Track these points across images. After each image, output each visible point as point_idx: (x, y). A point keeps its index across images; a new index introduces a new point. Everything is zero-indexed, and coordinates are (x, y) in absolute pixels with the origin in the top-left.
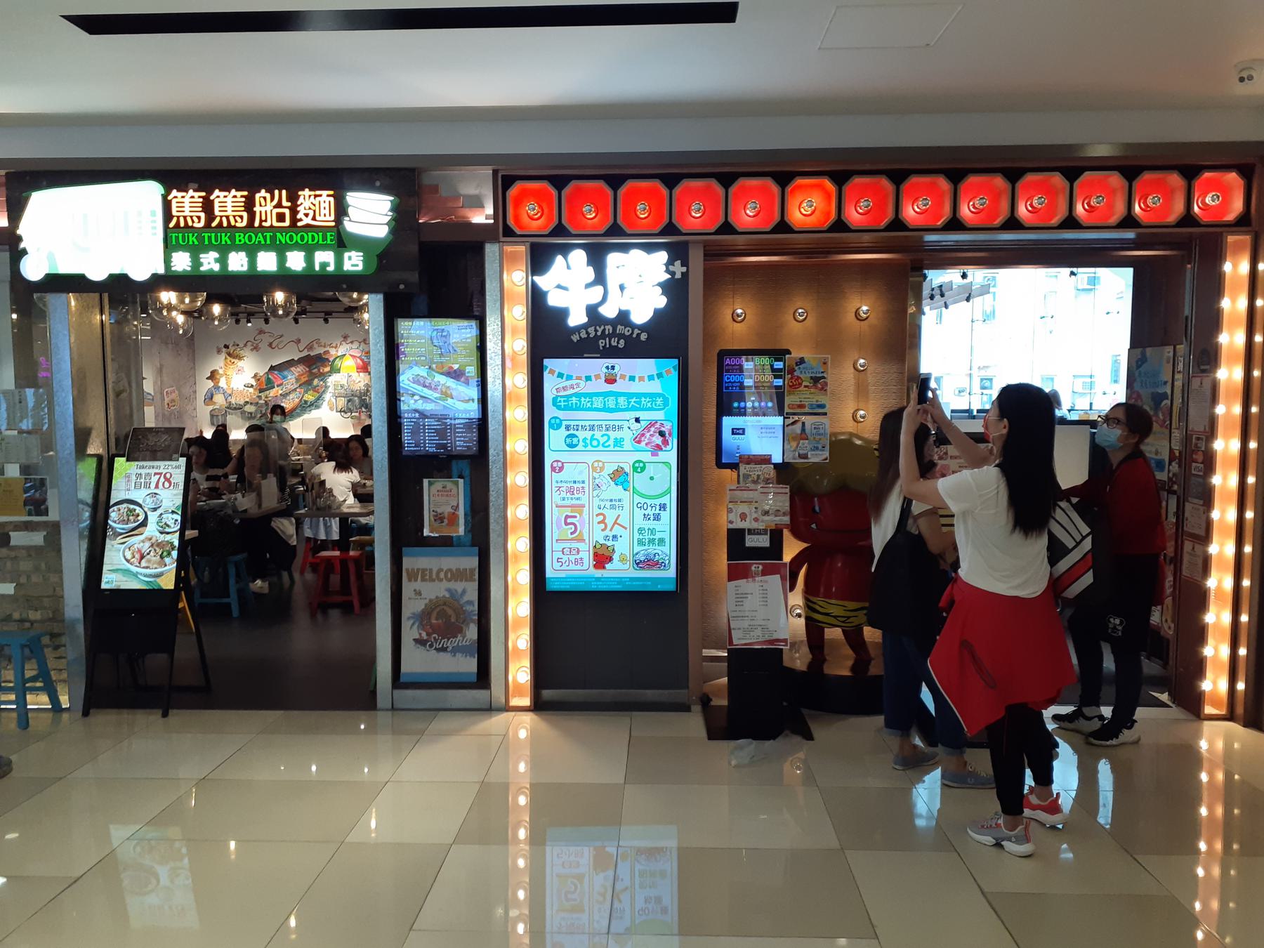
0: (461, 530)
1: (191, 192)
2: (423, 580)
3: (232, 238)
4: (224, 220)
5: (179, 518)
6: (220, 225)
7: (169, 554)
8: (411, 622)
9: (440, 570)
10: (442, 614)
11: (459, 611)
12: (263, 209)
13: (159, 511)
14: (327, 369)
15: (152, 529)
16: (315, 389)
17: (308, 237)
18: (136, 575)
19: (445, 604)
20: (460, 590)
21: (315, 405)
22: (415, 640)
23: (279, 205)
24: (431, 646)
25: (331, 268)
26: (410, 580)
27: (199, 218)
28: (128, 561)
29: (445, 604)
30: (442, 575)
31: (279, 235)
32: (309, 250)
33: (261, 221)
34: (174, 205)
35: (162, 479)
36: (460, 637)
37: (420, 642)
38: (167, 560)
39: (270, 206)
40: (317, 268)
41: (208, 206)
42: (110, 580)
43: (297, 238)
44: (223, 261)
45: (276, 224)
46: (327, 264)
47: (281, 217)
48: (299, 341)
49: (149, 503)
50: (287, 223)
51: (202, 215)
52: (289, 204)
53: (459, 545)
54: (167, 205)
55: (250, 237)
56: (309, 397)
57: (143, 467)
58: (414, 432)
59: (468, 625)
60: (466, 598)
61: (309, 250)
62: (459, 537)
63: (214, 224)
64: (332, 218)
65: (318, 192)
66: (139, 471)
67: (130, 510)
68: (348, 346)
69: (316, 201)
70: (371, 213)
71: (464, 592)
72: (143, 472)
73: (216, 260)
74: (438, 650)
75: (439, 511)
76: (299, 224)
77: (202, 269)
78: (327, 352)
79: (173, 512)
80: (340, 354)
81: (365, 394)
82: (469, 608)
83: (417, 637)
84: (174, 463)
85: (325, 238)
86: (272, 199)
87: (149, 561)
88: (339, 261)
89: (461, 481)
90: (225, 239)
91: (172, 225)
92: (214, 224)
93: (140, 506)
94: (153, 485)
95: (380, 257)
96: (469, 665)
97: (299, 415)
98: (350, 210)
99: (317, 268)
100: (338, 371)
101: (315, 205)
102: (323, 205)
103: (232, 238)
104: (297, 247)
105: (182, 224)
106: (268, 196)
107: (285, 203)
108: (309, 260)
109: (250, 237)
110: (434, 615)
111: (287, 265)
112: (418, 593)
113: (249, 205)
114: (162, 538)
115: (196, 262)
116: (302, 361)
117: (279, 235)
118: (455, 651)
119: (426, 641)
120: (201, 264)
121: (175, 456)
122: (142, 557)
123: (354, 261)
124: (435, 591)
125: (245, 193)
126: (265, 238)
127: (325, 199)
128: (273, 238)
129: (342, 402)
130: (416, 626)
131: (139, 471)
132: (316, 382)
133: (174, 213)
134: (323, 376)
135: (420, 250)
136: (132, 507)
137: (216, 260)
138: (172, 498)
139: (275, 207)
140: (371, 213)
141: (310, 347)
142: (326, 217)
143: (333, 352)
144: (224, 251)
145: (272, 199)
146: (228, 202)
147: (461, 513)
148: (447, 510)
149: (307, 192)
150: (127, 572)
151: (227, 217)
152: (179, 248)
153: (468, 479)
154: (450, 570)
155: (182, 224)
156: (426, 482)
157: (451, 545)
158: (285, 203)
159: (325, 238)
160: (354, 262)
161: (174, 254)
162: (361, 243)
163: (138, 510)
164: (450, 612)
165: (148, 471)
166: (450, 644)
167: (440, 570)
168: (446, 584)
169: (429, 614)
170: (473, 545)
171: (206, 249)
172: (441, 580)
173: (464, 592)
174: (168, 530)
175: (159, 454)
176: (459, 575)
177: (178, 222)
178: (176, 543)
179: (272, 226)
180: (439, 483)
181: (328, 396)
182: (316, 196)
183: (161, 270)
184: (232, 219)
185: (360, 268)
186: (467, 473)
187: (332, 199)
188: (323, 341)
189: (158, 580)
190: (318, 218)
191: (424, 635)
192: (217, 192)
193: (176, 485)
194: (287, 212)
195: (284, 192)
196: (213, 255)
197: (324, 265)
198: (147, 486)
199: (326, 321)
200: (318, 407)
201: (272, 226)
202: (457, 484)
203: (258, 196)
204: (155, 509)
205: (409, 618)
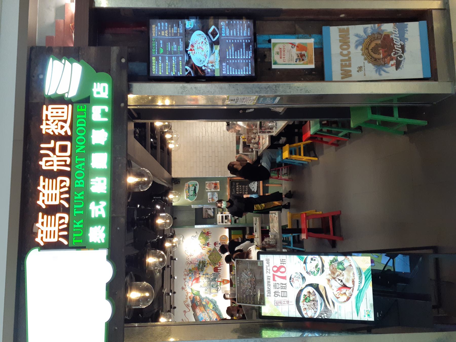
0: (311, 41)
1: (38, 225)
2: (350, 65)
3: (79, 190)
4: (63, 196)
5: (310, 257)
6: (67, 200)
7: (341, 263)
8: (382, 72)
9: (341, 54)
10: (375, 50)
11: (372, 38)
12: (56, 163)
13: (305, 275)
14: (198, 297)
15: (321, 280)
16: (207, 303)
17: (80, 126)
18: (360, 291)
19: (367, 49)
20: (357, 38)
21: (215, 304)
22: (397, 68)
23: (53, 150)
24: (401, 57)
25: (107, 109)
26: (351, 76)
27: (61, 218)
28: (348, 299)
29: (367, 49)
30: (345, 52)
31: (77, 151)
32: (91, 125)
33: (66, 165)
34: (48, 240)
35: (279, 274)
36: (393, 36)
37: (398, 65)
38: (346, 264)
39: (54, 158)
40: (106, 119)
41: (51, 210)
42: (366, 313)
43: (81, 136)
44: (97, 198)
45: (68, 153)
46: (103, 111)
47: (63, 149)
48: (185, 311)
49: (299, 284)
50: (68, 143)
51: (58, 215)
52: (53, 142)
53: (321, 43)
54: (49, 246)
55: (80, 175)
56: (211, 306)
57: (269, 291)
58: (237, 67)
59: (383, 31)
60: (362, 33)
61: (91, 125)
62: (315, 43)
63: (67, 205)
64: (65, 106)
65: (44, 118)
66: (272, 294)
67: (306, 299)
68: (187, 287)
69: (52, 119)
70: (62, 76)
71: (357, 35)
72: (273, 290)
73: (97, 204)
74: (403, 51)
75: (296, 57)
76: (69, 133)
77: (104, 216)
78: (190, 297)
79: (305, 263)
80: (191, 291)
81: (209, 279)
82: (369, 31)
83: (394, 67)
84: (265, 264)
85: (82, 113)
86: (48, 155)
87: (348, 280)
88: (100, 102)
89: (273, 41)
90: (79, 196)
91: (66, 242)
92: (67, 205)
93: (301, 291)
94: (283, 281)
95: (97, 70)
96: (414, 29)
97: (220, 311)
98: (60, 92)
99: (106, 119)
100: (198, 292)
101: (54, 120)
102: (55, 114)
103: (79, 190)
104: (88, 136)
105: (65, 233)
106: (45, 159)
107: (52, 145)
108: (98, 126)
109: (80, 175)
110: (376, 56)
111: (103, 143)
112: (360, 69)
113: (51, 175)
114: (327, 270)
115: (98, 221)
116: (194, 309)
117: (77, 151)
118: (402, 38)
119: (397, 60)
120: (100, 216)
121: (259, 264)
122: (345, 286)
123: (101, 90)
124: (357, 56)
125: (42, 178)
126: (80, 162)
127: (49, 112)
128: (80, 155)
129: (213, 290)
130: (384, 68)
131: (272, 294)
132: (204, 303)
133: (55, 240)
134: (201, 300)
135: (94, 45)
136: (302, 298)
137: (97, 204)
138: (293, 263)
139: (54, 153)
140: (62, 76)
141: (187, 306)
142: (65, 111)
143: (190, 295)
144: (90, 197)
145: (48, 155)
146: (49, 192)
147: (297, 41)
148: (295, 52)
149: (43, 127)
150: (358, 298)
151: (61, 193)
152: (85, 237)
153: (271, 36)
154: (341, 46)
155: (65, 233)
156: (274, 67)
157: (322, 49)
158: (52, 145)
159: (82, 113)
160: (102, 90)
161: (91, 240)
162: (86, 84)
163: (305, 292)
164: (373, 45)
165: (272, 287)
166: (398, 43)
167: (341, 54)
168: (352, 49)
169: (376, 60)
170: (321, 33)
171: (87, 212)
172: (349, 53)
173: (357, 35)
174: (320, 266)
175: (258, 278)
176: (344, 41)
177: (63, 236)
178: (331, 258)
179: (70, 156)
180: (275, 57)
181: (211, 297)
182: (47, 119)
183: (104, 253)
184: (63, 190)
185: (106, 85)
186: (266, 37)
187: (50, 107)
188: (185, 300)
189: (363, 271)
190: (65, 118)
191: (394, 61)
192: (40, 202)
193: (283, 261)
194: (59, 143)
195: (42, 146)
196: (92, 206)
197: (104, 114)
198: (284, 286)
199: (175, 308)
200: (216, 302)
201: (70, 156)
202: (275, 44)
203: (44, 168)
204: (304, 278)
205: (380, 75)
